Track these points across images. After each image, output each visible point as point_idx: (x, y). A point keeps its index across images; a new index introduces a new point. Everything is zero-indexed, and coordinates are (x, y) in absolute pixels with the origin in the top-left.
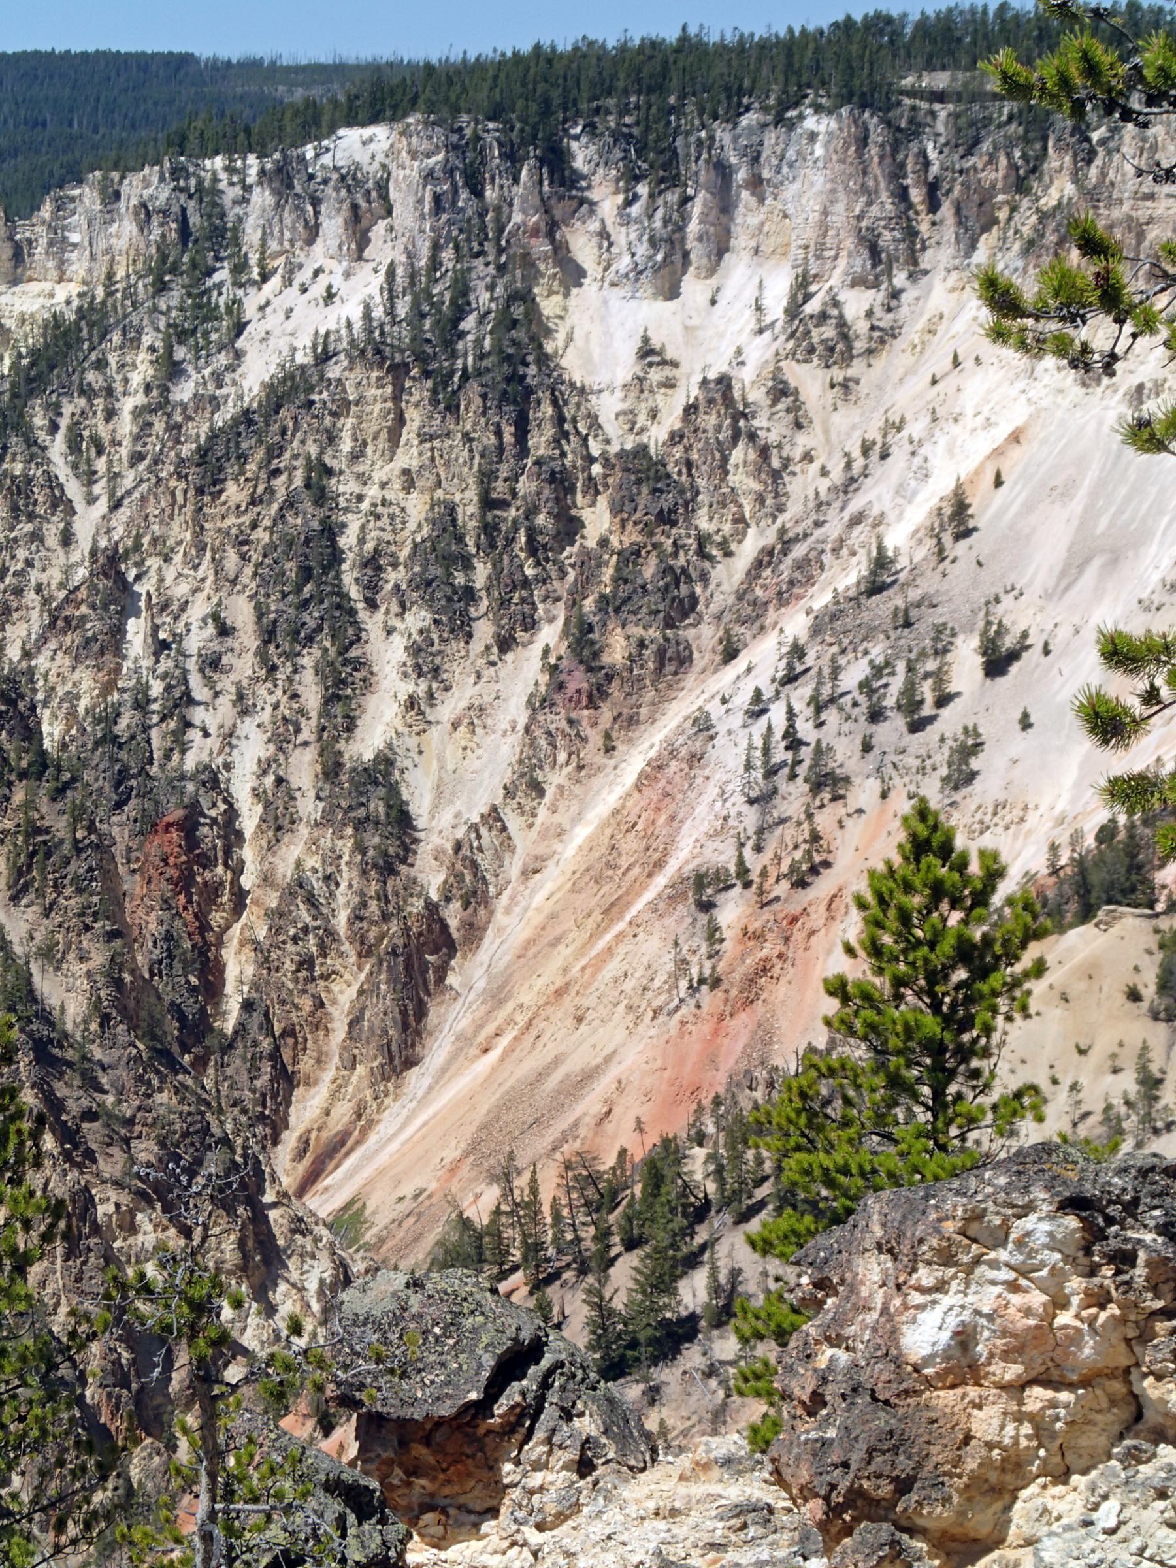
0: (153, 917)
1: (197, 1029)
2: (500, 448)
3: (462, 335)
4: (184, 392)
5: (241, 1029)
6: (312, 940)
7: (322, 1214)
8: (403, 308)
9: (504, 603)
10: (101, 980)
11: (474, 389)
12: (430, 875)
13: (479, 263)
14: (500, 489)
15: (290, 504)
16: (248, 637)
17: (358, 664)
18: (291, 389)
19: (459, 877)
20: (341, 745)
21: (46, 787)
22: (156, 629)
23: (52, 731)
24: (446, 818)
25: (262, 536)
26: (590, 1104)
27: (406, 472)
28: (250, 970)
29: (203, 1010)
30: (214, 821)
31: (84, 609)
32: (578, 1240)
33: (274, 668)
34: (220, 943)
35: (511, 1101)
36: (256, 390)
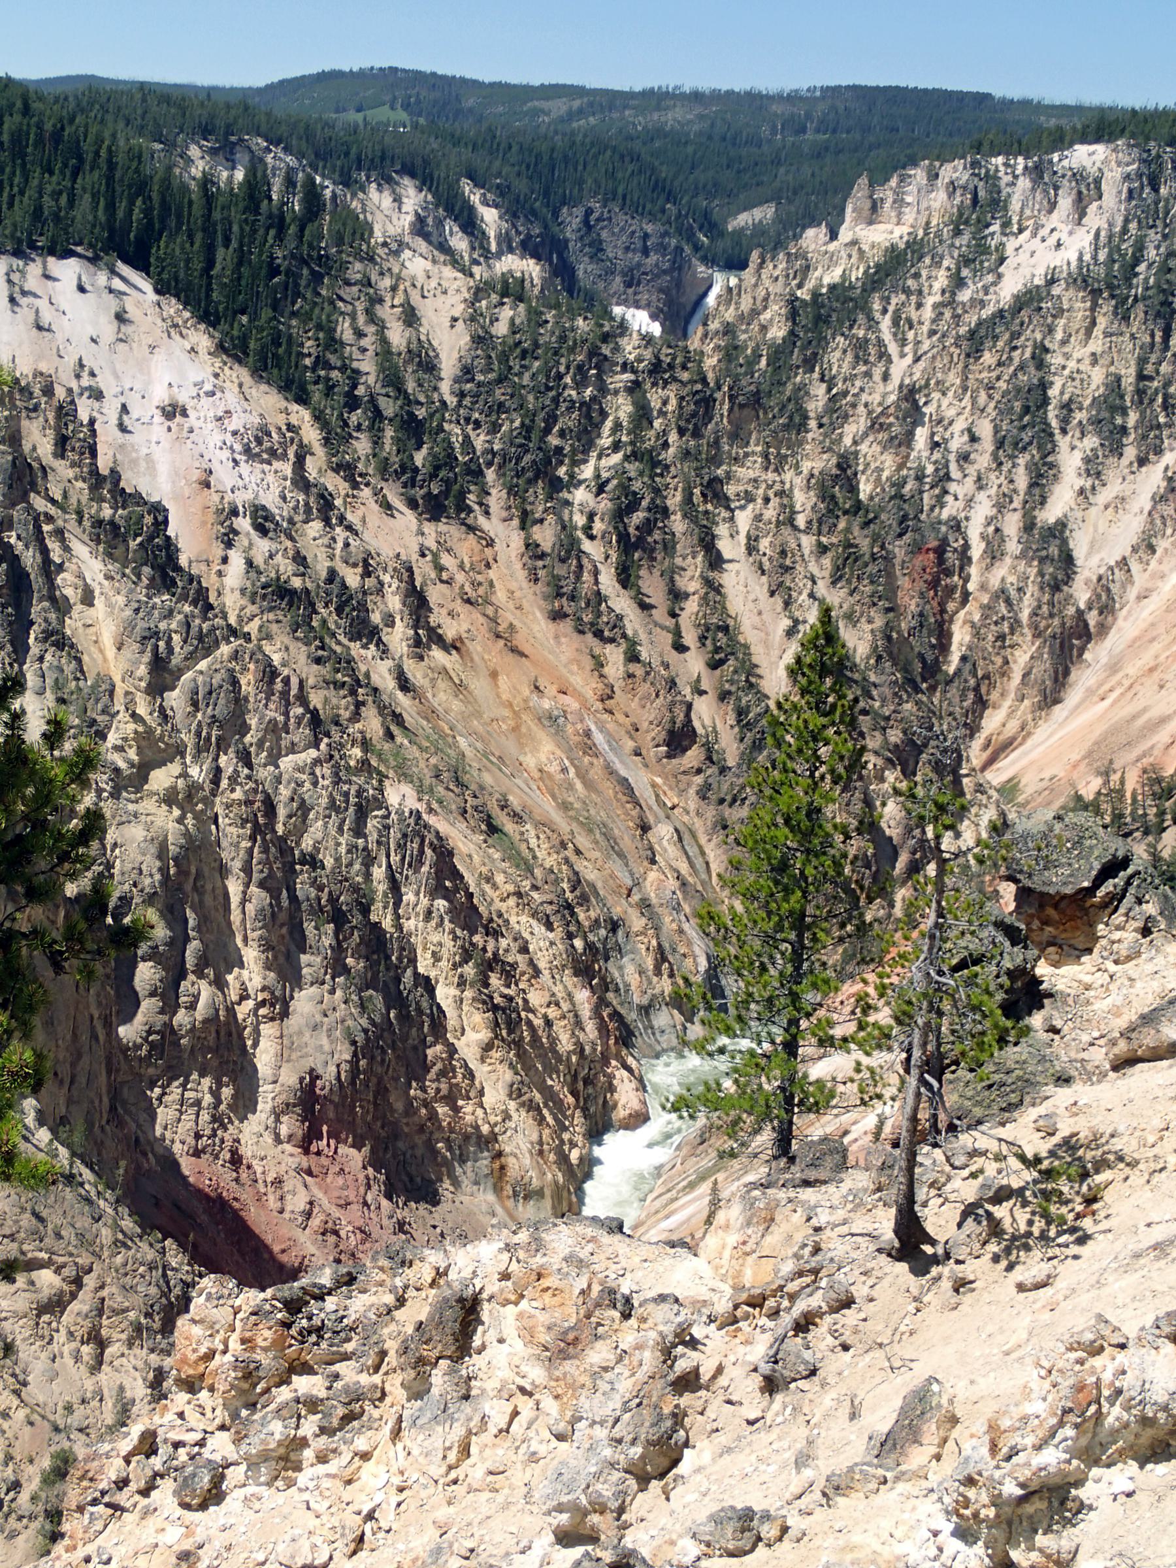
1: (932, 670)
2: (1153, 345)
3: (1136, 275)
4: (964, 296)
5: (958, 672)
7: (995, 783)
8: (1102, 256)
9: (1144, 437)
10: (879, 635)
11: (1141, 306)
12: (1081, 593)
13: (1152, 232)
14: (1149, 369)
15: (1022, 367)
17: (1051, 466)
19: (1099, 596)
21: (859, 520)
22: (933, 434)
23: (865, 489)
24: (1094, 561)
25: (1002, 385)
26: (1163, 736)
28: (967, 638)
32: (1145, 815)
34: (951, 621)
35: (1114, 730)
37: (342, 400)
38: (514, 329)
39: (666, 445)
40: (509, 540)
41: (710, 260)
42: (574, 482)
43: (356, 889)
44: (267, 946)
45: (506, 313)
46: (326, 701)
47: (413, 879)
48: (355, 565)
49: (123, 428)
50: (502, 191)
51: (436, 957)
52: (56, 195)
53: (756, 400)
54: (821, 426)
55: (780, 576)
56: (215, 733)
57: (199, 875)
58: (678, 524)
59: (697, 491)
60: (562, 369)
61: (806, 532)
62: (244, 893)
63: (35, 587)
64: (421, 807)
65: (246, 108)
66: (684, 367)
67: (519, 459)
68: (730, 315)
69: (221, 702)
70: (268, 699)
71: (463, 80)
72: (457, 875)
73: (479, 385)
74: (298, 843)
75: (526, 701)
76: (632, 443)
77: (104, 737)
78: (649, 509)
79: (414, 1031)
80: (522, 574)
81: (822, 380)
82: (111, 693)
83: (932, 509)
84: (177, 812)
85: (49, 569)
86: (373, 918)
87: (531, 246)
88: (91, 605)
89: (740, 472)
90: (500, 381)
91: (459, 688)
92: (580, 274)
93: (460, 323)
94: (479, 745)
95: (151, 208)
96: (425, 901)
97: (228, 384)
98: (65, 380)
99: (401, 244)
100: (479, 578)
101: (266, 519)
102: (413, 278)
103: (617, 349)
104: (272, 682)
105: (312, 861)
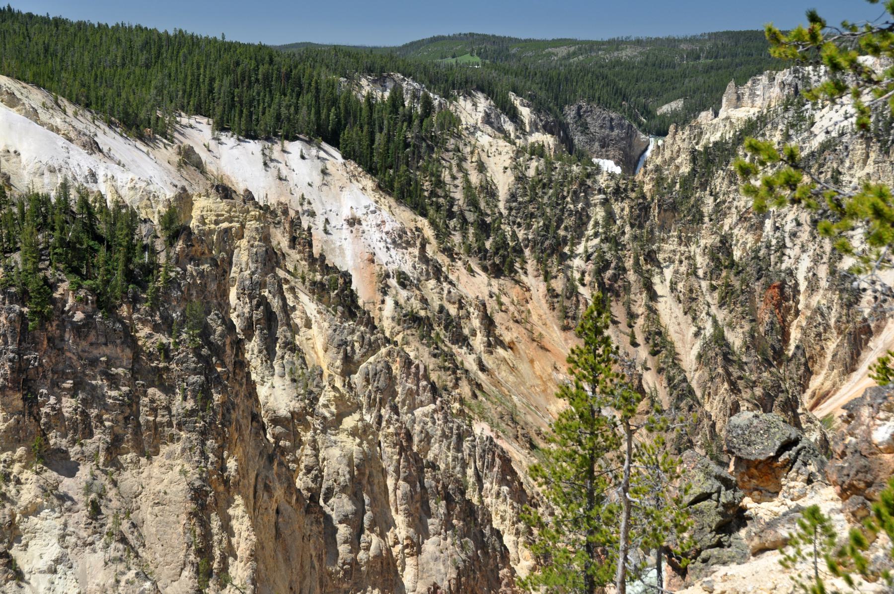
0: (767, 316)
1: (779, 354)
5: (794, 355)
6: (821, 327)
7: (819, 417)
10: (747, 335)
16: (807, 228)
18: (828, 146)
20: (837, 264)
22: (775, 222)
23: (737, 254)
27: (868, 174)
28: (799, 336)
29: (782, 348)
30: (790, 286)
31: (751, 215)
33: (815, 237)
34: (789, 325)
36: (817, 145)
37: (445, 213)
38: (538, 172)
39: (624, 233)
40: (537, 286)
41: (647, 131)
42: (573, 255)
43: (457, 481)
44: (408, 514)
45: (534, 164)
46: (439, 377)
47: (489, 475)
48: (454, 303)
49: (326, 232)
50: (532, 98)
51: (503, 519)
52: (288, 107)
53: (674, 207)
54: (711, 220)
55: (690, 304)
56: (378, 396)
57: (371, 475)
58: (631, 276)
59: (642, 258)
60: (565, 194)
61: (704, 278)
62: (396, 484)
63: (279, 318)
64: (493, 435)
65: (392, 58)
66: (633, 190)
67: (543, 243)
68: (659, 161)
69: (382, 379)
70: (407, 377)
71: (510, 39)
72: (514, 473)
73: (520, 203)
74: (425, 456)
75: (550, 375)
76: (605, 233)
77: (317, 400)
78: (615, 269)
79: (491, 561)
80: (545, 306)
81: (711, 195)
82: (321, 375)
83: (776, 264)
84: (358, 440)
85: (287, 310)
86: (467, 497)
87: (548, 128)
88: (310, 328)
89: (666, 247)
90: (530, 201)
91: (513, 369)
92: (576, 141)
93: (509, 171)
94: (524, 400)
95: (340, 113)
96: (496, 487)
97: (383, 207)
98: (295, 206)
99: (475, 128)
100: (522, 308)
101: (405, 279)
102: (483, 146)
103: (595, 181)
104: (409, 368)
105: (434, 466)
